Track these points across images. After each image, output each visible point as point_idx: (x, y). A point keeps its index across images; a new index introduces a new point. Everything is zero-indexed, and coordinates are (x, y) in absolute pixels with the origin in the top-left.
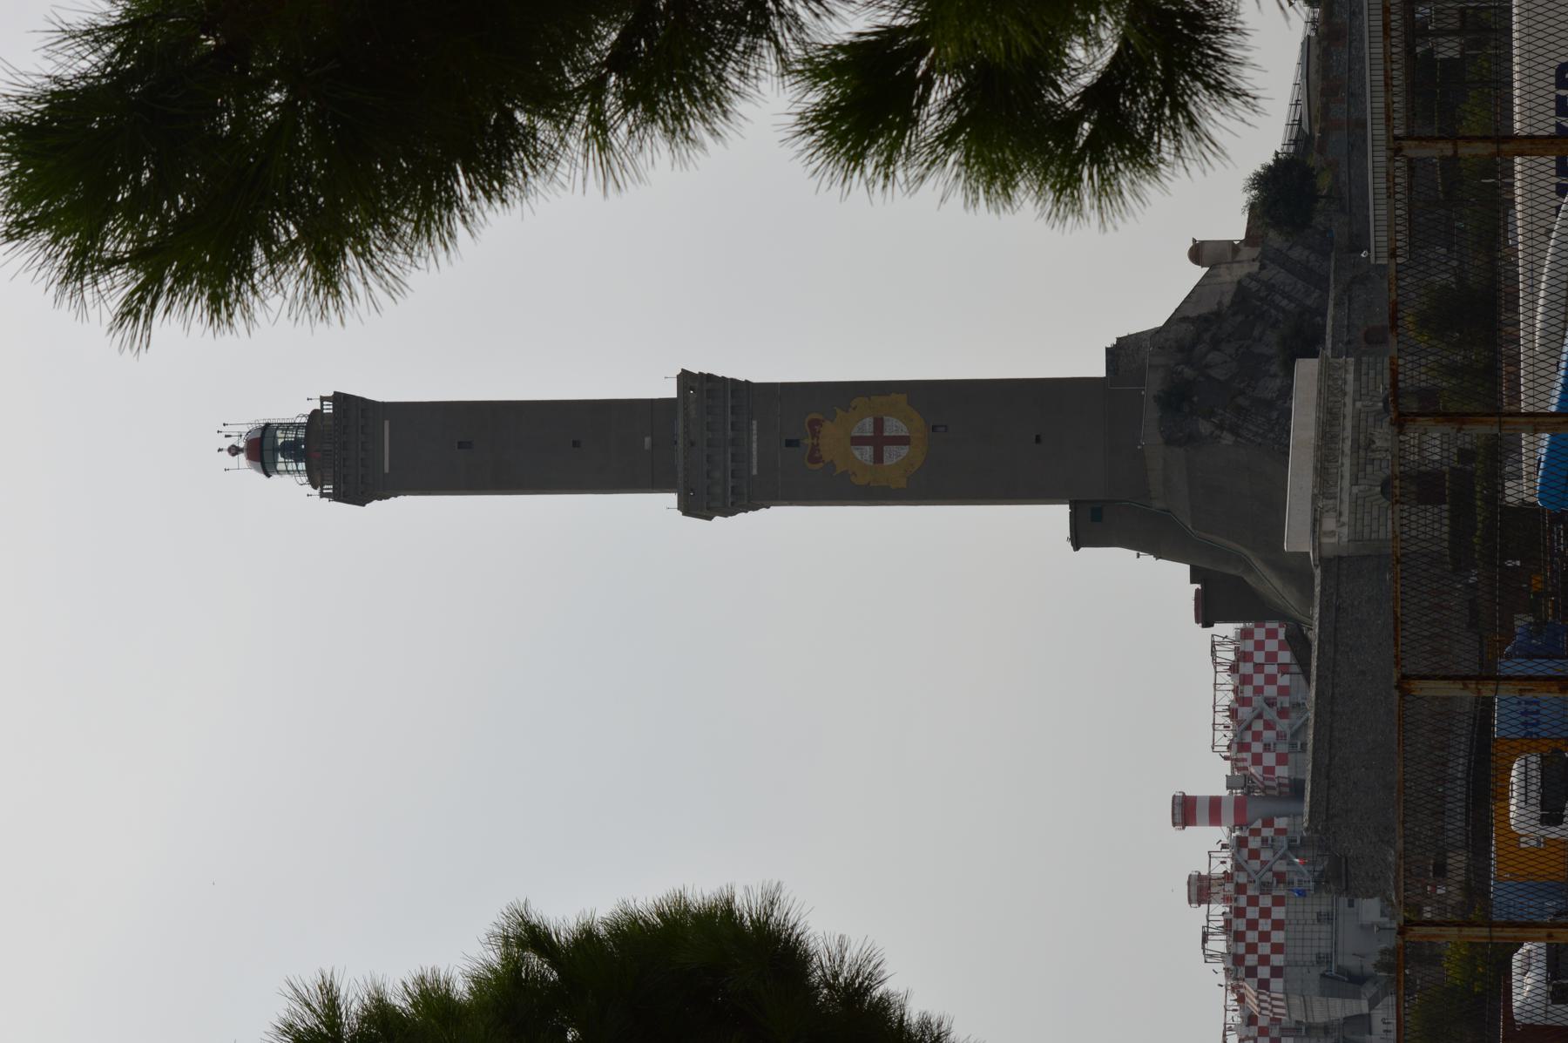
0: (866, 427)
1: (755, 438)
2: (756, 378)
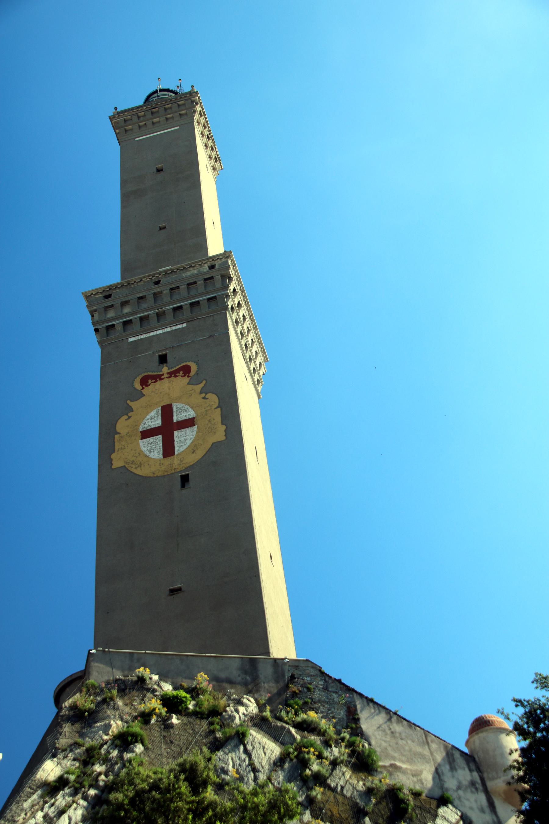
1: (168, 329)
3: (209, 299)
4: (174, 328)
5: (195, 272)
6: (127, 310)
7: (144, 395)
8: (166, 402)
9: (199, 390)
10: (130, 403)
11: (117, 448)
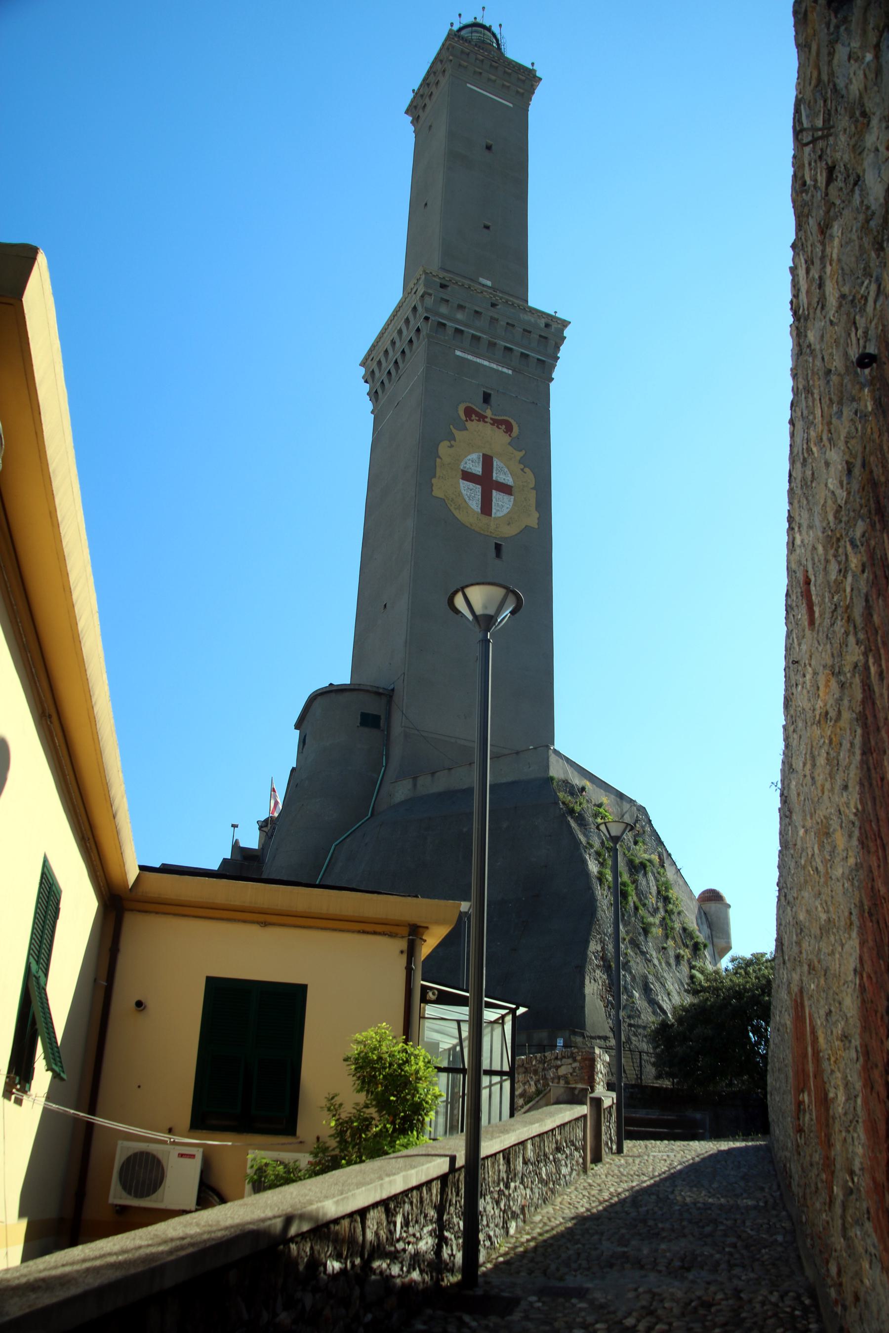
0: (501, 474)
1: (494, 366)
2: (555, 389)
3: (538, 359)
4: (500, 368)
5: (533, 320)
6: (460, 316)
7: (466, 429)
8: (489, 453)
9: (518, 458)
10: (454, 431)
11: (437, 475)
